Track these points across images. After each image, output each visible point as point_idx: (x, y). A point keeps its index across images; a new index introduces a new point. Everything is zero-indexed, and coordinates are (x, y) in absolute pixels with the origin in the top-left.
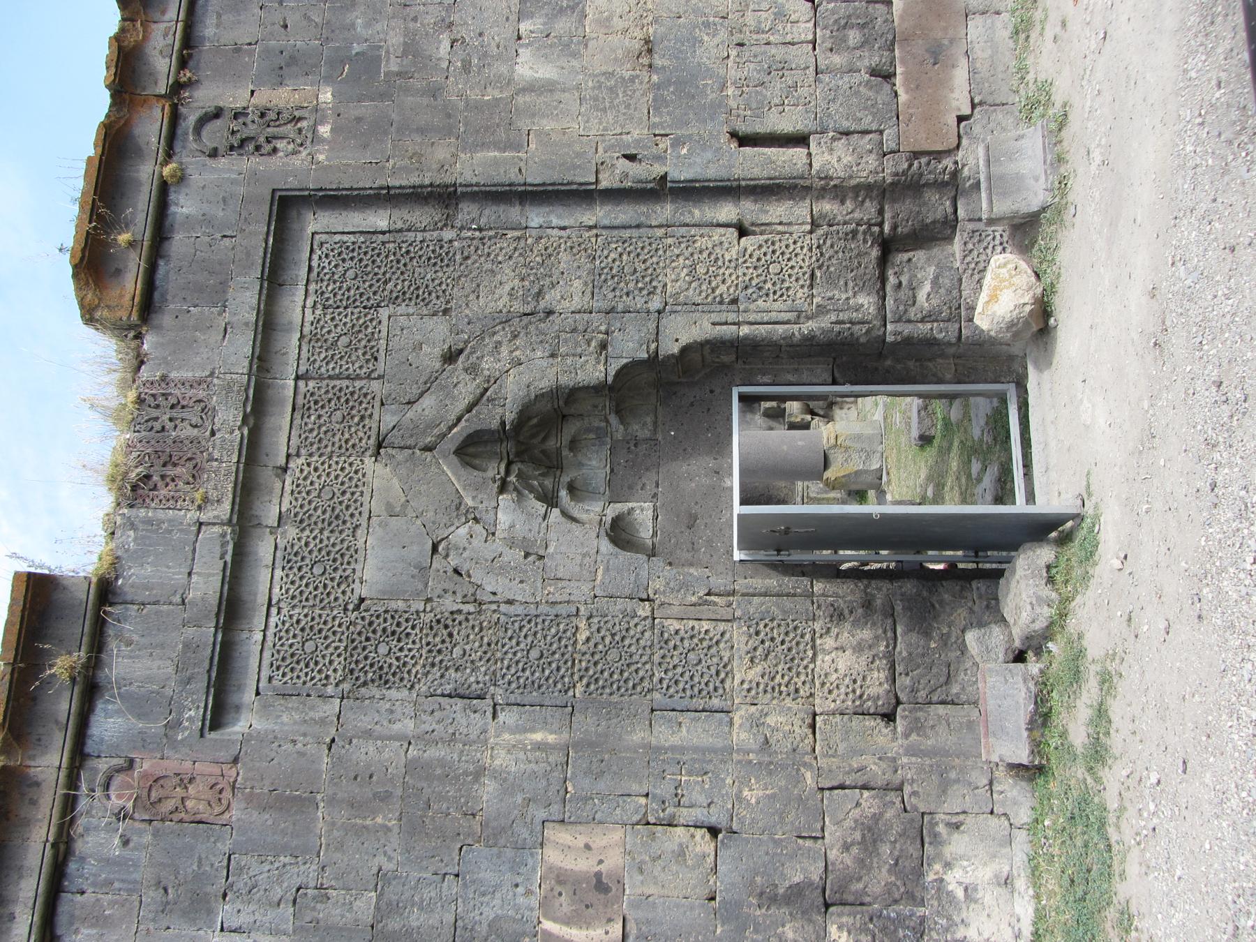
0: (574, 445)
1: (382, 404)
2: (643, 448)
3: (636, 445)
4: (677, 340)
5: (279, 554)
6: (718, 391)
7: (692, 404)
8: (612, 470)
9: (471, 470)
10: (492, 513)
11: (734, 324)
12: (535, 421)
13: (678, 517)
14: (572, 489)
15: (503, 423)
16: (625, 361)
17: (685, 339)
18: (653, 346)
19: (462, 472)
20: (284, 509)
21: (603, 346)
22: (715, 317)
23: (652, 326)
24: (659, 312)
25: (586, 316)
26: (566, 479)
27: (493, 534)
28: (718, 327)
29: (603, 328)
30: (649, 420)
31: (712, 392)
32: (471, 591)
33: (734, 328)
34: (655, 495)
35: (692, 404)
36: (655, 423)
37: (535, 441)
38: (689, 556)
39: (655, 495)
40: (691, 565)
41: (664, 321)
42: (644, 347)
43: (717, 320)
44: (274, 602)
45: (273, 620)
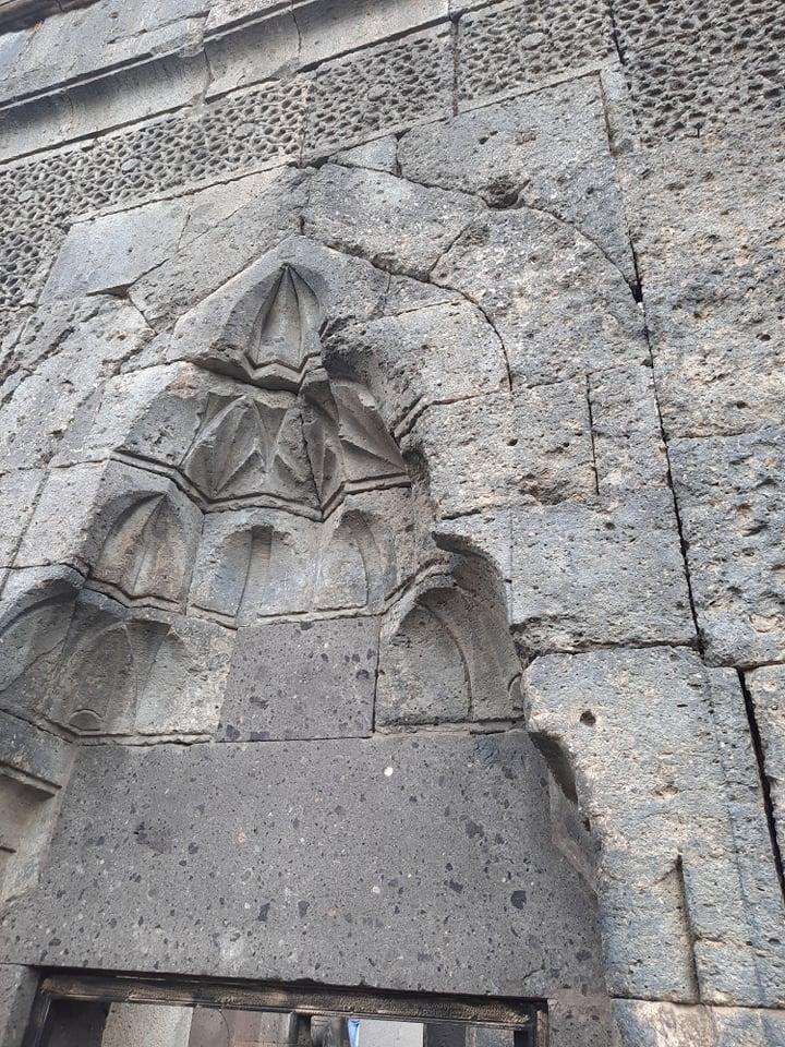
0: (358, 522)
1: (399, 136)
2: (357, 693)
3: (363, 673)
4: (588, 718)
5: (166, 117)
6: (524, 922)
7: (474, 830)
8: (306, 626)
9: (257, 305)
10: (157, 358)
11: (696, 979)
12: (367, 401)
13: (172, 798)
14: (261, 537)
15: (340, 324)
16: (501, 557)
17: (592, 756)
18: (561, 638)
19: (246, 288)
20: (228, 96)
21: (553, 496)
22: (713, 877)
23: (638, 624)
24: (700, 644)
25: (649, 424)
26: (281, 522)
27: (117, 372)
28: (664, 894)
29: (615, 478)
30: (425, 702)
31: (518, 899)
32: (25, 363)
33: (677, 976)
34: (233, 734)
35: (474, 830)
36: (415, 722)
37: (346, 430)
38: (78, 823)
39: (233, 734)
40: (55, 839)
41: (660, 661)
42: (554, 609)
43: (700, 890)
44: (100, 139)
45: (77, 147)
